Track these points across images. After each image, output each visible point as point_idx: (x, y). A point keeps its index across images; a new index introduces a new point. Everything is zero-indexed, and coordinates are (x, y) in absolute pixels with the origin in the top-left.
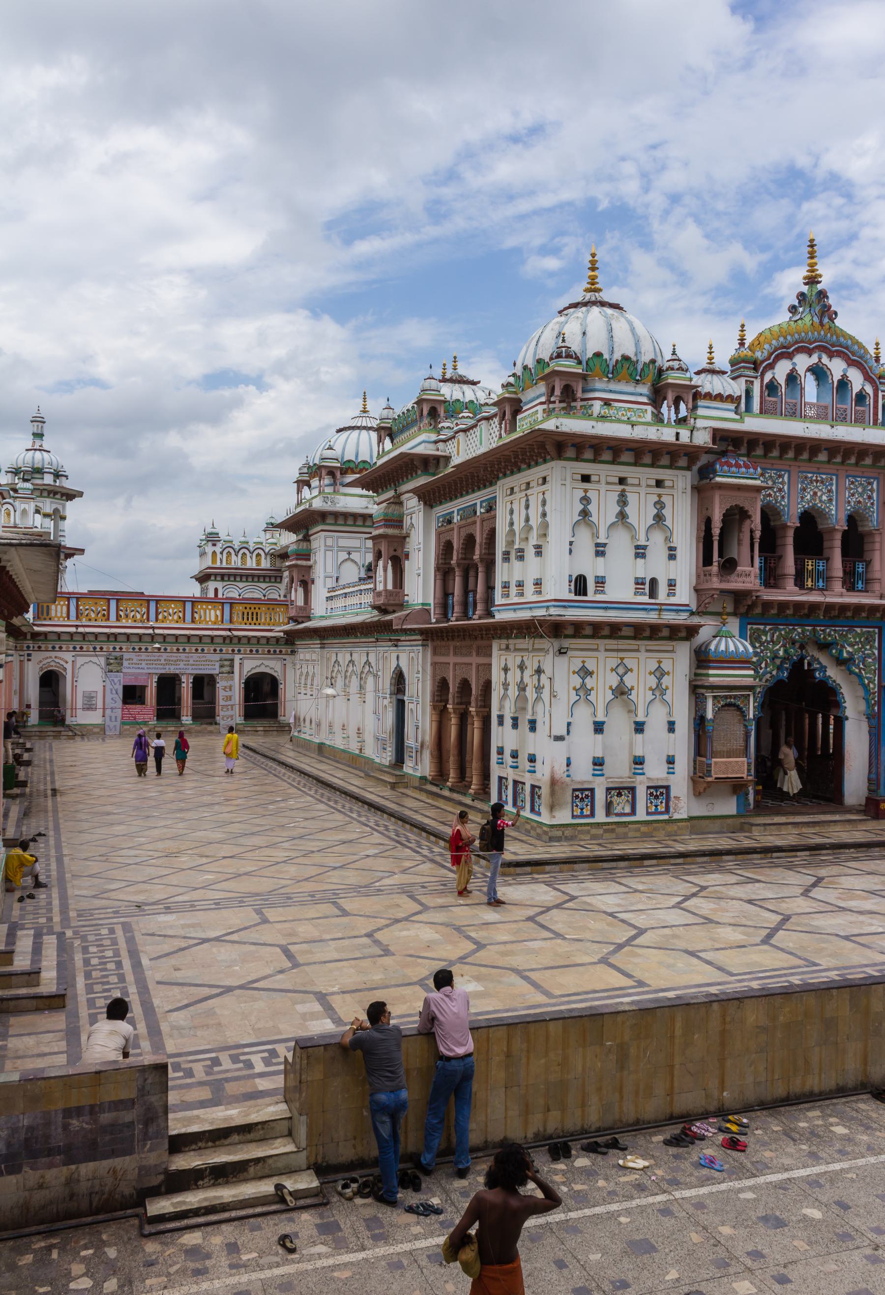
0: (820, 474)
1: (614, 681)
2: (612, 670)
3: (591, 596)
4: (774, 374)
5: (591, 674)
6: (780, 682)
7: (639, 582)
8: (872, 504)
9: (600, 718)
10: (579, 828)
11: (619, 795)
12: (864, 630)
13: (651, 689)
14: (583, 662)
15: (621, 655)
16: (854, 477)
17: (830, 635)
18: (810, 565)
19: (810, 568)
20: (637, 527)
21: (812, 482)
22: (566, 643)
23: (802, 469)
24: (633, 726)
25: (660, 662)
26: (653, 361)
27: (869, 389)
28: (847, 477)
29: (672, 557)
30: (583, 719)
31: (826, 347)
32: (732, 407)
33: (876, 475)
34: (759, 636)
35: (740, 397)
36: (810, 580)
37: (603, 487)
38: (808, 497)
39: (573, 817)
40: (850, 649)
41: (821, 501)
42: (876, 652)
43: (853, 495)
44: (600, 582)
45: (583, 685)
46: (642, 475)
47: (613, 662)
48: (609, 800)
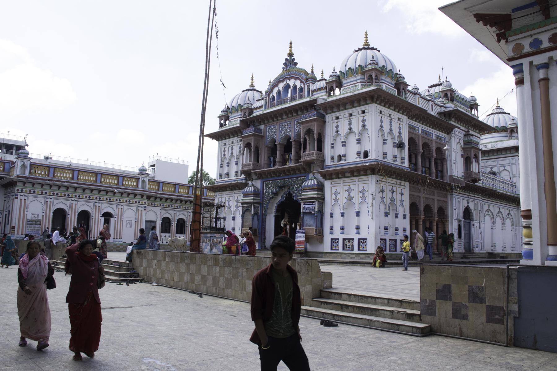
18: (288, 157)
27: (302, 86)
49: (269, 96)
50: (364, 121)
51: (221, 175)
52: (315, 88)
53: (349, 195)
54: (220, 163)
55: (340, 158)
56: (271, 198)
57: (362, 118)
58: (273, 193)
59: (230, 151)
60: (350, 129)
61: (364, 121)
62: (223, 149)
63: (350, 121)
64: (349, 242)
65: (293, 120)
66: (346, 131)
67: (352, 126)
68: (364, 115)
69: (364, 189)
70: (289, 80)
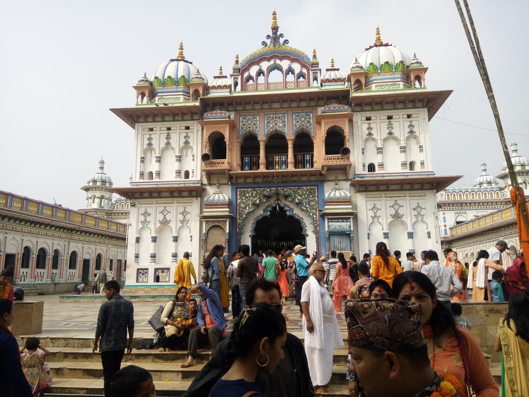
0: (277, 114)
1: (161, 217)
2: (160, 213)
4: (249, 73)
5: (149, 215)
6: (265, 218)
7: (179, 172)
8: (310, 125)
9: (154, 235)
10: (138, 287)
11: (163, 272)
12: (308, 188)
13: (180, 221)
14: (146, 209)
17: (286, 191)
18: (277, 159)
19: (277, 160)
21: (273, 118)
22: (137, 202)
23: (266, 113)
24: (172, 239)
25: (185, 208)
26: (183, 77)
27: (305, 71)
28: (294, 113)
29: (193, 160)
30: (147, 237)
31: (277, 56)
32: (228, 90)
33: (311, 111)
34: (245, 194)
35: (230, 86)
36: (277, 166)
37: (158, 132)
38: (271, 126)
39: (137, 281)
40: (300, 198)
41: (279, 127)
42: (316, 199)
43: (298, 122)
44: (159, 174)
46: (178, 126)
47: (161, 209)
48: (157, 274)
49: (242, 75)
51: (142, 175)
52: (327, 77)
53: (397, 212)
55: (371, 168)
56: (249, 213)
57: (409, 123)
58: (254, 204)
59: (164, 141)
60: (390, 133)
61: (411, 126)
62: (147, 136)
63: (390, 124)
65: (290, 112)
66: (385, 135)
67: (393, 131)
69: (418, 206)
70: (281, 60)
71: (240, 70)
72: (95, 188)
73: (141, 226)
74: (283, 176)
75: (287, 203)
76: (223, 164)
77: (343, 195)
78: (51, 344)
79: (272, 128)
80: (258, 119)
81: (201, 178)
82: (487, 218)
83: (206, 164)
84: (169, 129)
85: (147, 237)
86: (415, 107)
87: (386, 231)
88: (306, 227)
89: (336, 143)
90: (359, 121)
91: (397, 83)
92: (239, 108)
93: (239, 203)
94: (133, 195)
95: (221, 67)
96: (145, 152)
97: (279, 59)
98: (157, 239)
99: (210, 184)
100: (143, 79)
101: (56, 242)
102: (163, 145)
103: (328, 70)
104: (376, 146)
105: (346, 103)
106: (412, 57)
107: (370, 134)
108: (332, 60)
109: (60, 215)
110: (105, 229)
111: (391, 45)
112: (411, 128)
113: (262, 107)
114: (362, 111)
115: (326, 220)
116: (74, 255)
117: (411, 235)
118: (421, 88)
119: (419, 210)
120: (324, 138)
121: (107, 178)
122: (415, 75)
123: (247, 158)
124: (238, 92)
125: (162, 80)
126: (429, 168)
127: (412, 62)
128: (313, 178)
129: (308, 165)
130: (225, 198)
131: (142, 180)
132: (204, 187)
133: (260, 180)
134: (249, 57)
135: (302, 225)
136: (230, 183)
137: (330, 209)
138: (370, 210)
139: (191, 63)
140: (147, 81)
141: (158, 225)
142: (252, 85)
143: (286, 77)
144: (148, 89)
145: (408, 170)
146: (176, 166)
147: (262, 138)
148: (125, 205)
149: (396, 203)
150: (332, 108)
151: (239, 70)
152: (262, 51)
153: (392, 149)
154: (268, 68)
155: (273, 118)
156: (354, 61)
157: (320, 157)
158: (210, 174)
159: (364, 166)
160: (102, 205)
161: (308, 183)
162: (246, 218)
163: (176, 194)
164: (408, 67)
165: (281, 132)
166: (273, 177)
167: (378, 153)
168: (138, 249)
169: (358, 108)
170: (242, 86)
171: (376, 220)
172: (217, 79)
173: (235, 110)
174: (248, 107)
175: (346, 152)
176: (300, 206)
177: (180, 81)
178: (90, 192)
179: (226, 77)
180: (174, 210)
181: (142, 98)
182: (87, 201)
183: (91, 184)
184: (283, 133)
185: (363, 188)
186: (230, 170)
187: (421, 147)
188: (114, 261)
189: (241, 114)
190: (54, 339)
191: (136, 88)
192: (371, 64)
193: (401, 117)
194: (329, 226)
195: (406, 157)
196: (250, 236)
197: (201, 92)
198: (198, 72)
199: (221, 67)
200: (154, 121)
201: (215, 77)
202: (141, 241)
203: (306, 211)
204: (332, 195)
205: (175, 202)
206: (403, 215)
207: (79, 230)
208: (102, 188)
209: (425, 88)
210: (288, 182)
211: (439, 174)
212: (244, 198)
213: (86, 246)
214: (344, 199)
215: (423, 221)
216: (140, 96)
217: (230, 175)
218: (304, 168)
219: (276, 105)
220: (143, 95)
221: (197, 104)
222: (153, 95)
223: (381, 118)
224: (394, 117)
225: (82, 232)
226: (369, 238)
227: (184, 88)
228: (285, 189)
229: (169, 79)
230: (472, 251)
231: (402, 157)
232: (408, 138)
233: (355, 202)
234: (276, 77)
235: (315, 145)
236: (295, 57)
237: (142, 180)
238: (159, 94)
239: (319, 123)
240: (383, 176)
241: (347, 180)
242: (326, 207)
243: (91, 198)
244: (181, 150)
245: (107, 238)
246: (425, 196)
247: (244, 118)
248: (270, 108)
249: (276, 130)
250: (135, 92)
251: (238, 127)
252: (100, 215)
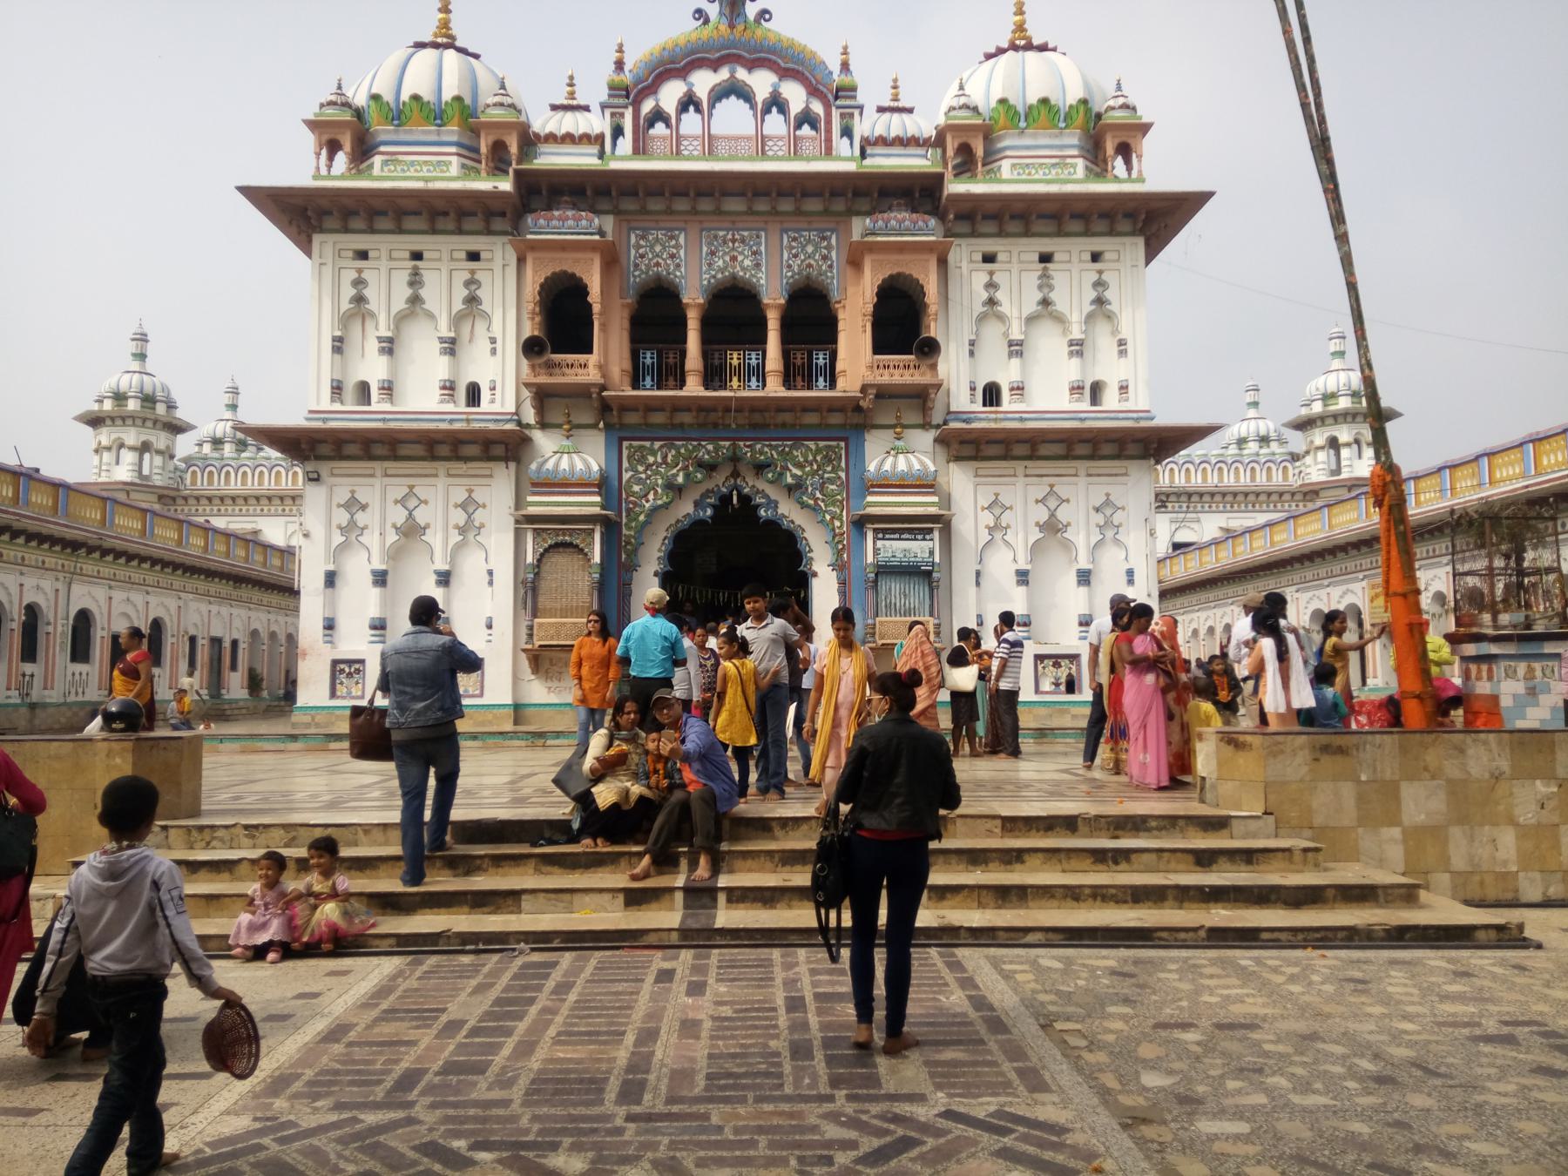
1: (399, 515)
2: (396, 502)
3: (374, 407)
4: (657, 101)
5: (364, 507)
6: (699, 524)
7: (449, 387)
8: (831, 266)
12: (822, 444)
13: (457, 527)
14: (353, 492)
15: (411, 481)
16: (796, 230)
18: (734, 359)
19: (735, 362)
20: (436, 313)
21: (725, 242)
22: (324, 468)
23: (706, 225)
24: (434, 577)
25: (470, 491)
26: (458, 99)
27: (817, 108)
29: (494, 352)
30: (357, 570)
32: (595, 150)
34: (644, 457)
35: (600, 139)
36: (735, 379)
37: (384, 264)
38: (721, 263)
39: (333, 695)
40: (799, 473)
41: (743, 269)
42: (843, 475)
43: (796, 256)
44: (388, 389)
45: (352, 524)
46: (444, 249)
49: (637, 104)
50: (1099, 284)
51: (337, 389)
52: (879, 131)
53: (1052, 515)
54: (328, 332)
55: (992, 394)
56: (655, 509)
57: (1095, 277)
58: (670, 486)
59: (402, 292)
60: (1045, 302)
61: (1099, 284)
63: (1045, 276)
64: (1057, 665)
66: (1031, 305)
67: (1053, 296)
68: (1098, 266)
69: (1108, 502)
71: (631, 92)
72: (123, 419)
73: (338, 539)
74: (753, 410)
75: (761, 485)
76: (585, 369)
77: (917, 466)
78: (246, 841)
79: (722, 270)
80: (682, 240)
81: (518, 406)
82: (1256, 535)
83: (533, 367)
84: (417, 256)
85: (357, 570)
86: (1112, 232)
87: (1022, 565)
88: (811, 551)
89: (902, 322)
90: (964, 264)
91: (1069, 160)
92: (629, 205)
93: (628, 481)
94: (313, 449)
95: (571, 78)
96: (345, 320)
97: (744, 66)
98: (389, 578)
99: (543, 425)
100: (333, 98)
101: (30, 582)
102: (399, 304)
103: (881, 110)
104: (1006, 334)
105: (929, 208)
106: (1112, 92)
107: (991, 302)
108: (895, 80)
109: (40, 498)
110: (171, 545)
111: (1054, 50)
112: (1100, 289)
113: (694, 208)
114: (974, 234)
115: (870, 535)
116: (83, 621)
117: (1084, 578)
118: (1130, 180)
119: (1108, 512)
120: (870, 308)
121: (159, 388)
122: (1117, 141)
123: (648, 355)
124: (622, 158)
125: (393, 105)
126: (1139, 400)
127: (1111, 103)
128: (836, 419)
129: (821, 379)
130: (588, 467)
131: (337, 407)
132: (527, 432)
133: (687, 418)
134: (656, 52)
135: (801, 546)
136: (601, 425)
137: (880, 503)
138: (983, 509)
139: (477, 57)
140: (346, 105)
141: (392, 537)
142: (664, 138)
143: (763, 121)
144: (350, 132)
145: (1085, 405)
146: (441, 368)
147: (693, 297)
148: (284, 474)
149: (1052, 492)
150: (893, 223)
151: (627, 89)
152: (694, 36)
153: (1049, 345)
154: (712, 90)
155: (725, 242)
156: (954, 89)
157: (856, 360)
158: (543, 397)
159: (973, 389)
160: (146, 471)
161: (821, 432)
162: (647, 523)
163: (444, 450)
164: (1099, 116)
165: (749, 282)
166: (727, 410)
167: (1011, 355)
168: (331, 603)
169: (964, 227)
170: (636, 140)
171: (998, 535)
172: (560, 114)
173: (616, 212)
174: (655, 205)
175: (930, 349)
176: (798, 494)
177: (449, 112)
178: (104, 430)
179: (586, 109)
180: (438, 496)
181: (331, 158)
182: (96, 459)
183: (108, 405)
184: (754, 286)
185: (968, 450)
186: (603, 388)
187: (1122, 343)
188: (200, 642)
189: (634, 224)
190: (256, 827)
191: (313, 125)
192: (1003, 101)
193: (1075, 258)
194: (876, 551)
195: (1083, 369)
196: (656, 574)
197: (514, 149)
198: (503, 87)
199: (571, 78)
200: (372, 230)
201: (555, 108)
202: (338, 582)
203: (815, 509)
204: (887, 466)
205: (442, 472)
206: (1069, 524)
207: (98, 548)
208: (144, 420)
209: (1143, 181)
210: (765, 426)
211: (1166, 417)
212: (641, 469)
213: (119, 596)
214: (919, 478)
215: (1117, 542)
216: (324, 152)
217: (603, 399)
218: (810, 388)
219: (734, 205)
220: (333, 147)
221: (506, 185)
222: (363, 150)
223: (1024, 257)
224: (1057, 257)
225: (105, 552)
226: (978, 584)
227: (460, 134)
228: (758, 446)
229: (414, 104)
230: (1209, 623)
231: (1072, 370)
232: (1090, 318)
233: (945, 487)
234: (733, 118)
235: (841, 326)
236: (790, 63)
237: (337, 407)
238: (382, 149)
239: (855, 263)
240: (1021, 419)
241: (926, 426)
242: (870, 499)
243: (109, 449)
244: (457, 320)
245: (179, 572)
246: (1126, 474)
247: (643, 237)
248: (718, 212)
249: (734, 277)
250: (309, 139)
251: (624, 261)
252: (147, 501)
